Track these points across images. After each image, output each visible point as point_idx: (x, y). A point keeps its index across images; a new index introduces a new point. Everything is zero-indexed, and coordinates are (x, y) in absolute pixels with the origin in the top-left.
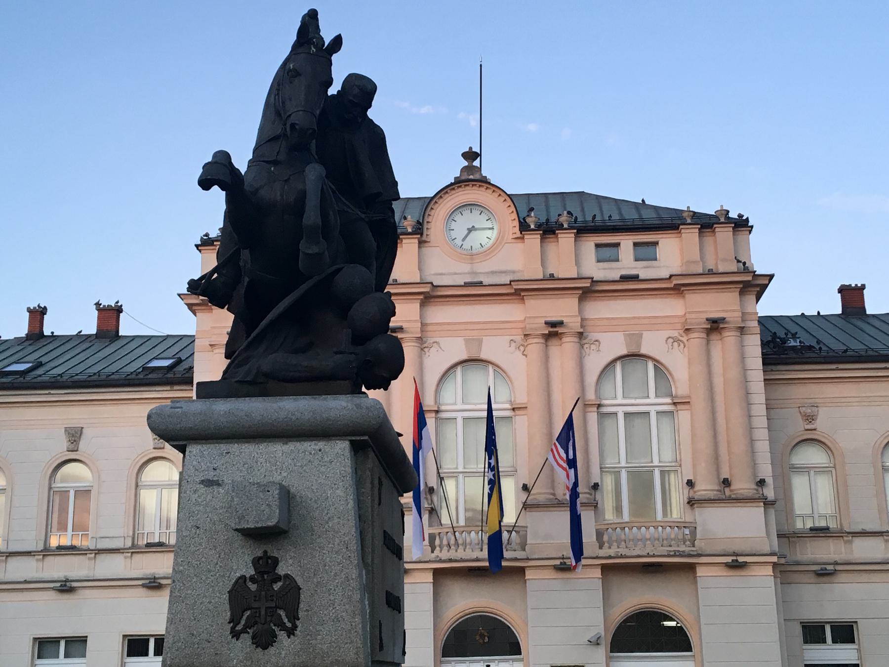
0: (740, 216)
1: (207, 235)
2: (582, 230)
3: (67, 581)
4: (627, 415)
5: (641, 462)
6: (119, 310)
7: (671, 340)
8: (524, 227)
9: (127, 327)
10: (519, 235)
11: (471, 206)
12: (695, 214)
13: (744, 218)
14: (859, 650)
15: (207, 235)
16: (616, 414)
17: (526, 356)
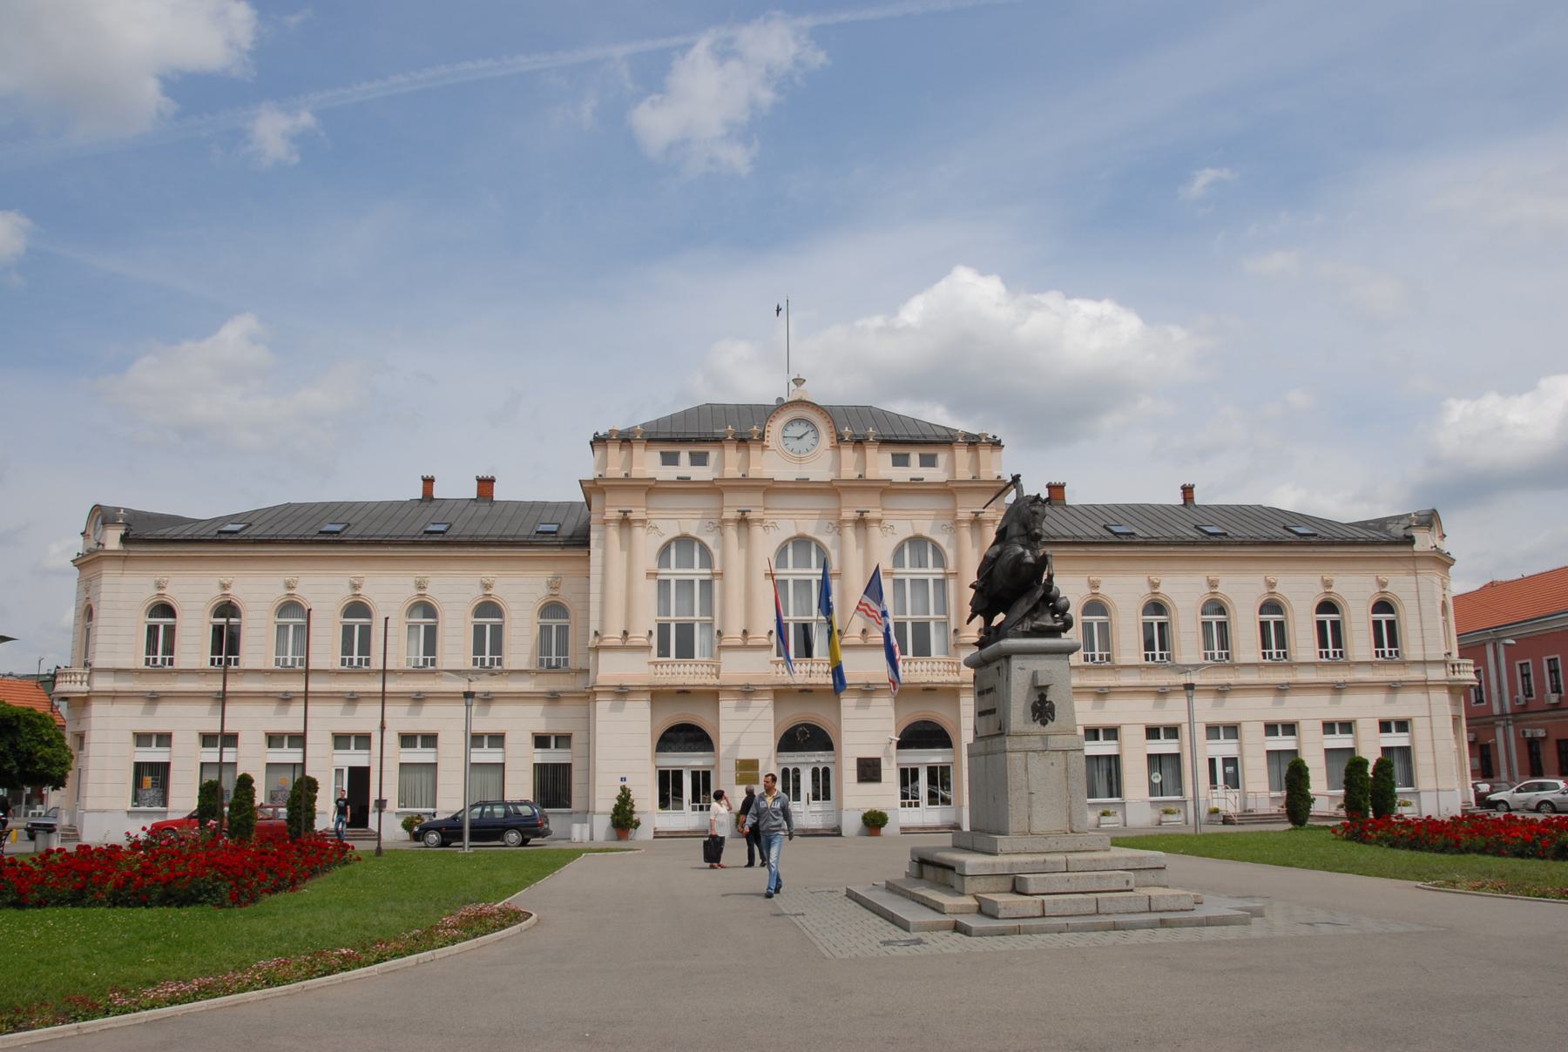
0: (995, 437)
1: (597, 434)
2: (885, 442)
3: (489, 693)
5: (920, 617)
6: (492, 481)
7: (944, 527)
8: (840, 439)
9: (499, 494)
10: (836, 444)
11: (800, 420)
12: (967, 436)
13: (998, 439)
15: (597, 434)
16: (903, 580)
17: (840, 535)
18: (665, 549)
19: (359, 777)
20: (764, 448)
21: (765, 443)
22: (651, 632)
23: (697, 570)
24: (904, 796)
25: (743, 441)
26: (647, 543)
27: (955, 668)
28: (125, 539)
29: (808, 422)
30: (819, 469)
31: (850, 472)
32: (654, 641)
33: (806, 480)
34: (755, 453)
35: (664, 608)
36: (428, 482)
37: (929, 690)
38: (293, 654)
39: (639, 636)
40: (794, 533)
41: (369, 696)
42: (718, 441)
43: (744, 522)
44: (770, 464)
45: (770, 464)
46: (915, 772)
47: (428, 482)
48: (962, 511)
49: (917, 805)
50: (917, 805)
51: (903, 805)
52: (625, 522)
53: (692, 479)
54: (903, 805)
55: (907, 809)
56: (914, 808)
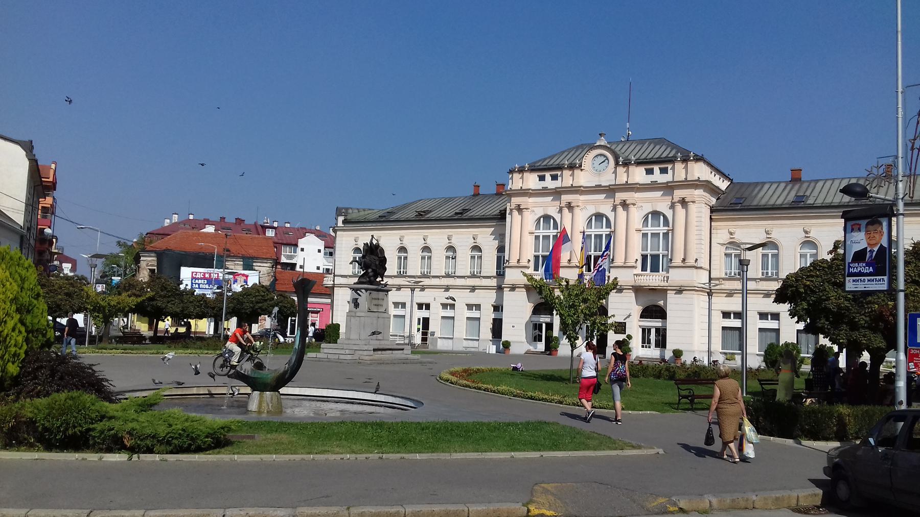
2: (639, 163)
4: (652, 234)
8: (617, 164)
14: (779, 323)
18: (539, 219)
19: (426, 322)
20: (582, 170)
21: (582, 168)
22: (529, 261)
23: (552, 230)
24: (643, 342)
25: (572, 167)
26: (530, 218)
27: (666, 279)
28: (344, 222)
29: (604, 156)
30: (607, 179)
31: (622, 178)
32: (532, 264)
33: (600, 186)
34: (577, 172)
35: (537, 250)
36: (477, 187)
37: (653, 290)
38: (403, 269)
39: (524, 262)
40: (594, 212)
41: (406, 287)
42: (560, 168)
43: (570, 207)
44: (583, 178)
45: (583, 178)
46: (649, 330)
47: (477, 187)
48: (677, 197)
49: (650, 347)
50: (650, 347)
51: (643, 347)
52: (519, 209)
53: (549, 188)
54: (643, 347)
55: (645, 349)
56: (648, 349)
